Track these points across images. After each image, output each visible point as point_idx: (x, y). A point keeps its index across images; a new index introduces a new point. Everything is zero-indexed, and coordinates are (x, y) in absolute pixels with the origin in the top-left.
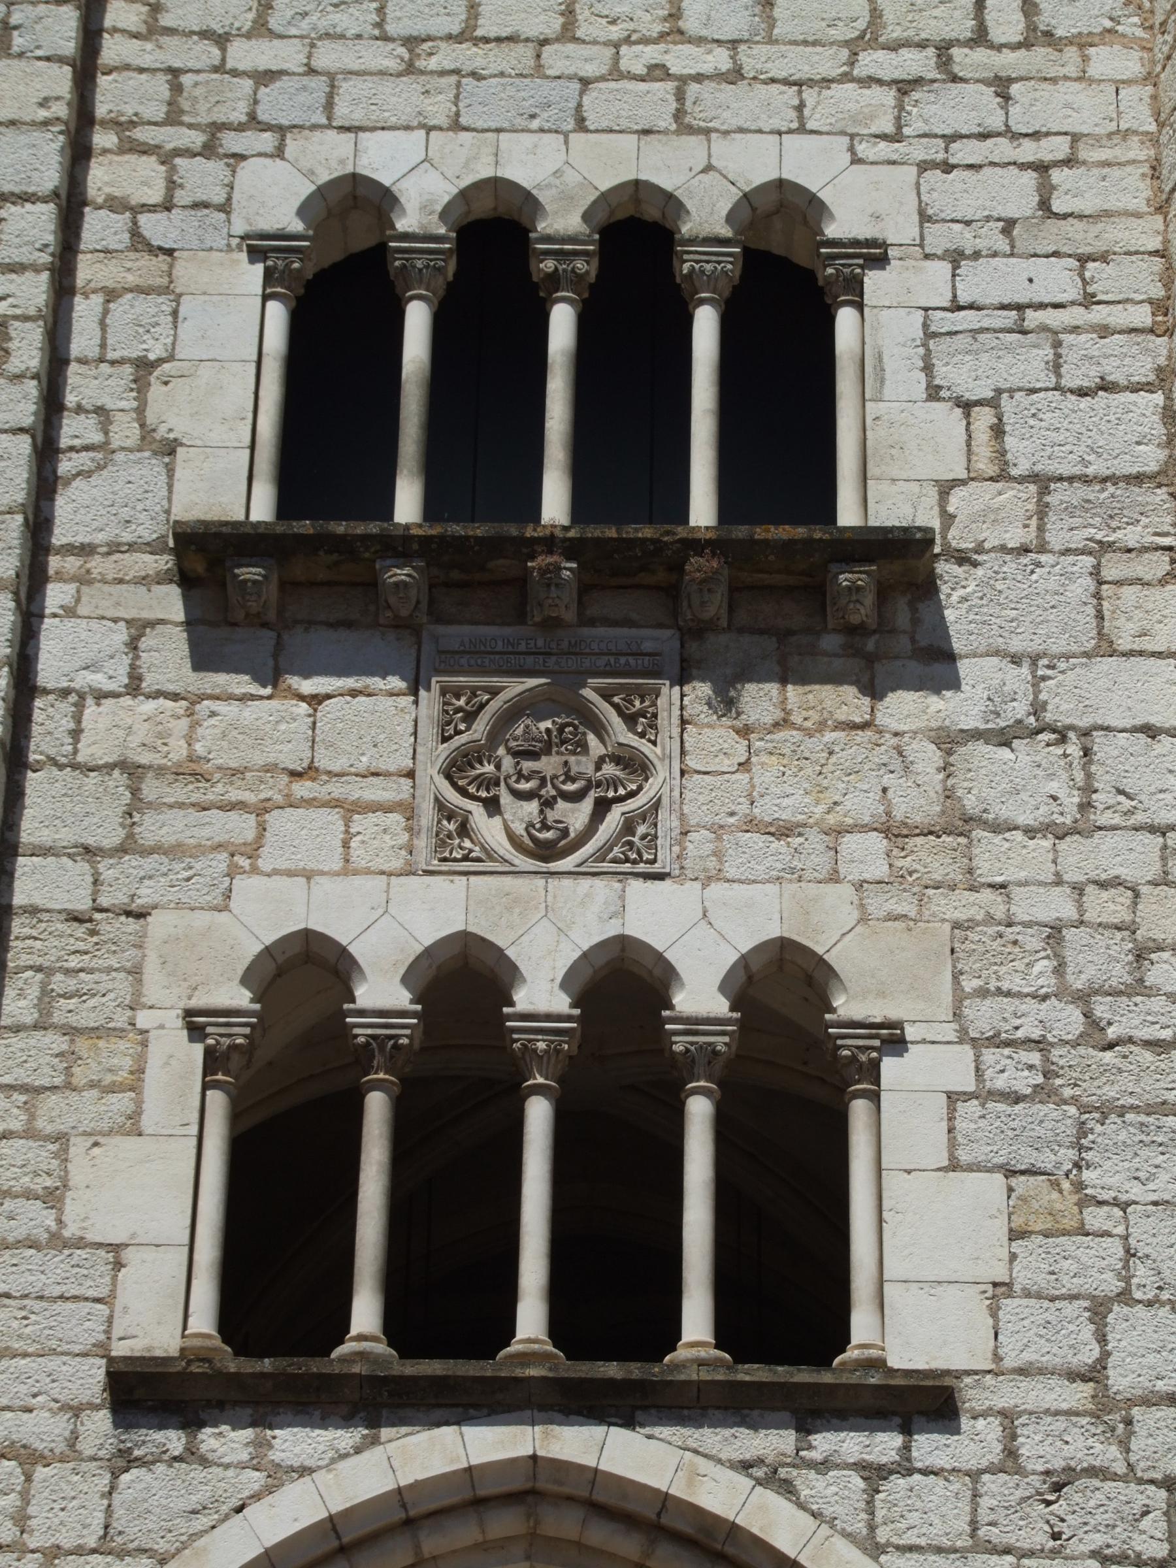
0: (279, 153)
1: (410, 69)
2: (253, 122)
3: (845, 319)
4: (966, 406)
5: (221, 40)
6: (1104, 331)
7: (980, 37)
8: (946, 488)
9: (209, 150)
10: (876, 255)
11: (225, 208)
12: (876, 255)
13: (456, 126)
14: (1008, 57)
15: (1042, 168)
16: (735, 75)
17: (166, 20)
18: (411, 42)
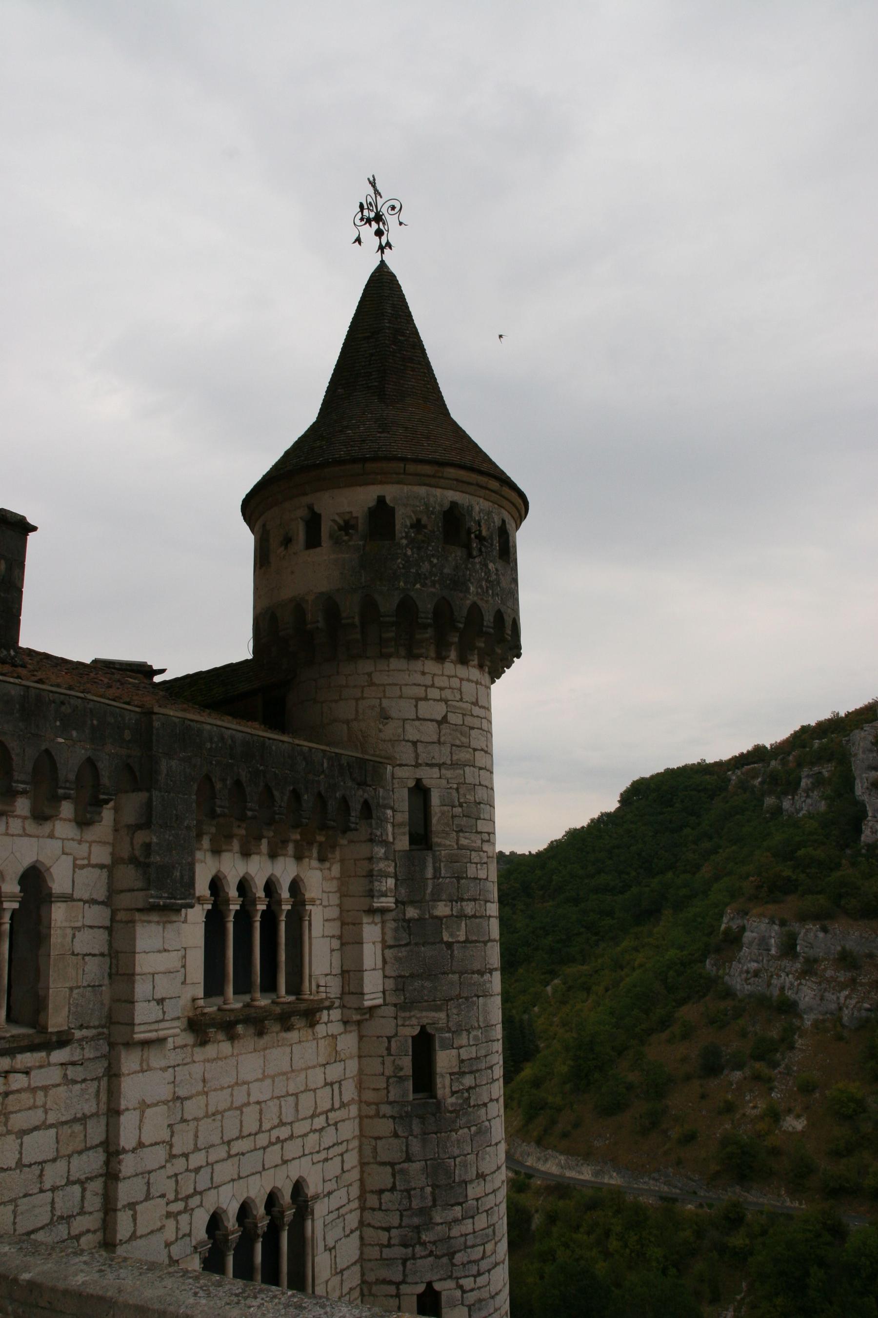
0: (201, 1205)
1: (230, 1156)
2: (196, 1192)
3: (309, 1222)
4: (330, 1250)
5: (186, 1156)
6: (351, 1211)
7: (333, 1109)
8: (327, 1282)
9: (185, 1210)
10: (316, 1197)
11: (189, 1235)
12: (316, 1197)
13: (240, 1178)
14: (338, 1112)
15: (342, 1155)
16: (291, 1137)
17: (175, 1151)
18: (229, 1143)
